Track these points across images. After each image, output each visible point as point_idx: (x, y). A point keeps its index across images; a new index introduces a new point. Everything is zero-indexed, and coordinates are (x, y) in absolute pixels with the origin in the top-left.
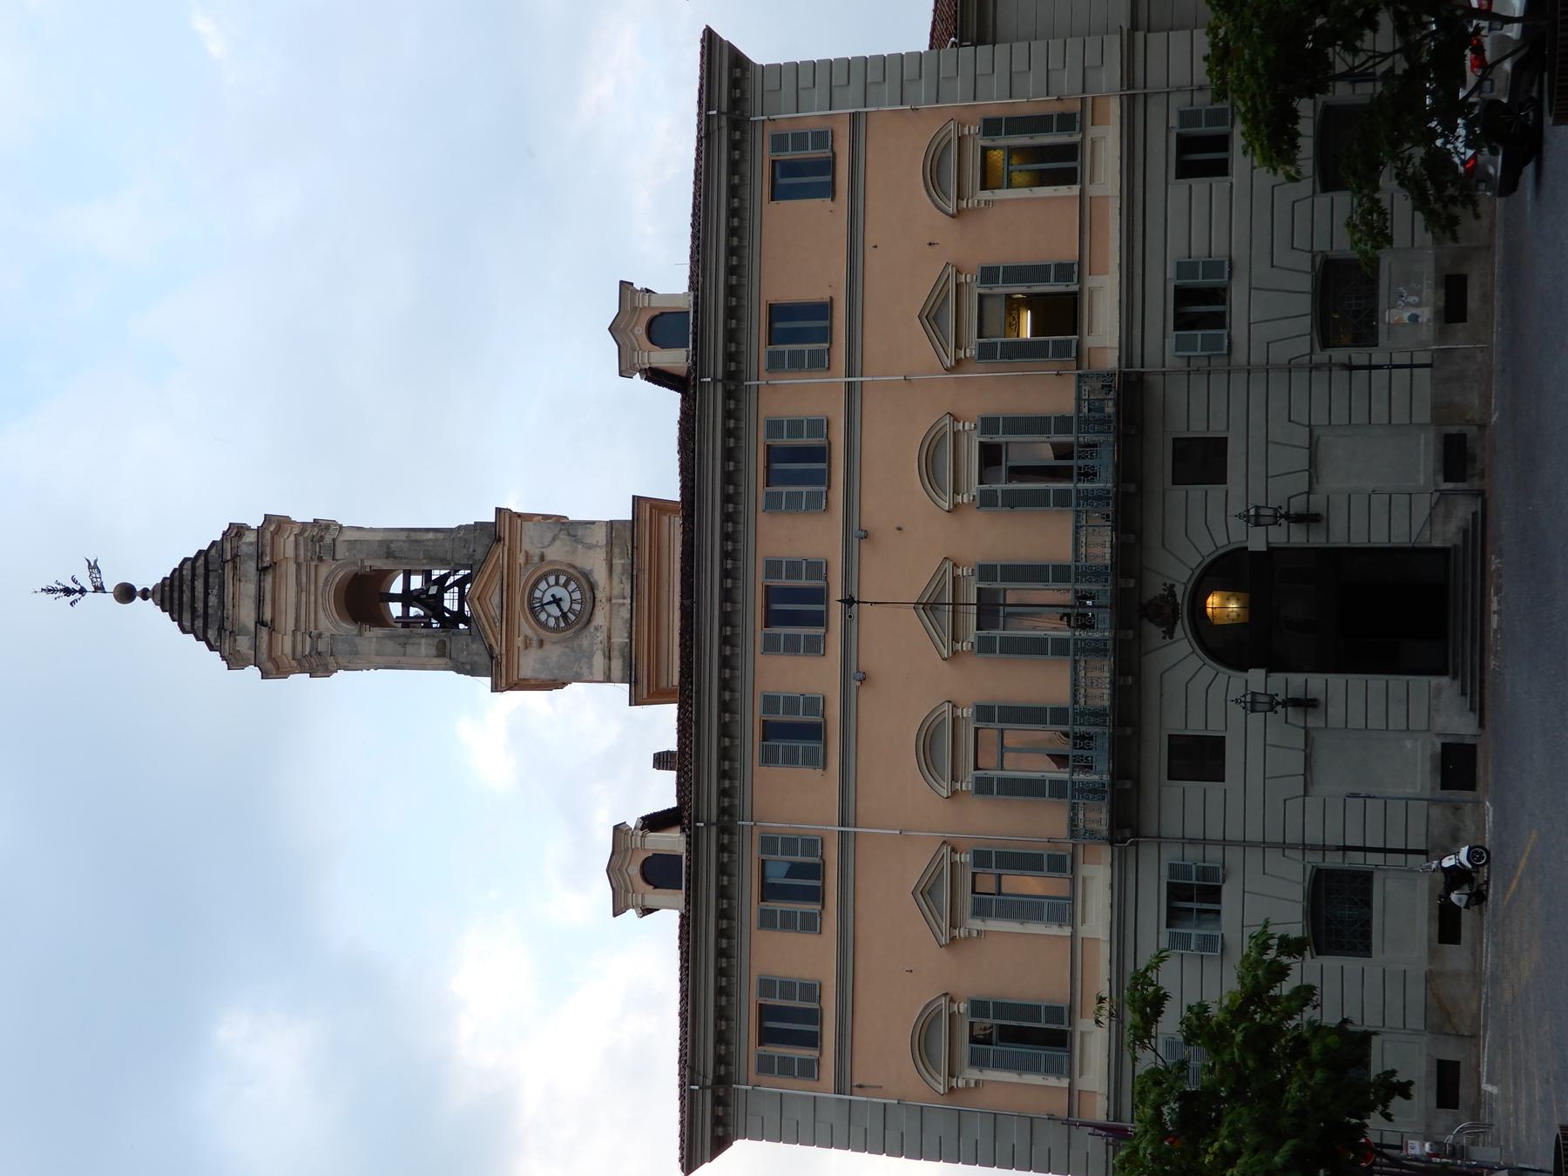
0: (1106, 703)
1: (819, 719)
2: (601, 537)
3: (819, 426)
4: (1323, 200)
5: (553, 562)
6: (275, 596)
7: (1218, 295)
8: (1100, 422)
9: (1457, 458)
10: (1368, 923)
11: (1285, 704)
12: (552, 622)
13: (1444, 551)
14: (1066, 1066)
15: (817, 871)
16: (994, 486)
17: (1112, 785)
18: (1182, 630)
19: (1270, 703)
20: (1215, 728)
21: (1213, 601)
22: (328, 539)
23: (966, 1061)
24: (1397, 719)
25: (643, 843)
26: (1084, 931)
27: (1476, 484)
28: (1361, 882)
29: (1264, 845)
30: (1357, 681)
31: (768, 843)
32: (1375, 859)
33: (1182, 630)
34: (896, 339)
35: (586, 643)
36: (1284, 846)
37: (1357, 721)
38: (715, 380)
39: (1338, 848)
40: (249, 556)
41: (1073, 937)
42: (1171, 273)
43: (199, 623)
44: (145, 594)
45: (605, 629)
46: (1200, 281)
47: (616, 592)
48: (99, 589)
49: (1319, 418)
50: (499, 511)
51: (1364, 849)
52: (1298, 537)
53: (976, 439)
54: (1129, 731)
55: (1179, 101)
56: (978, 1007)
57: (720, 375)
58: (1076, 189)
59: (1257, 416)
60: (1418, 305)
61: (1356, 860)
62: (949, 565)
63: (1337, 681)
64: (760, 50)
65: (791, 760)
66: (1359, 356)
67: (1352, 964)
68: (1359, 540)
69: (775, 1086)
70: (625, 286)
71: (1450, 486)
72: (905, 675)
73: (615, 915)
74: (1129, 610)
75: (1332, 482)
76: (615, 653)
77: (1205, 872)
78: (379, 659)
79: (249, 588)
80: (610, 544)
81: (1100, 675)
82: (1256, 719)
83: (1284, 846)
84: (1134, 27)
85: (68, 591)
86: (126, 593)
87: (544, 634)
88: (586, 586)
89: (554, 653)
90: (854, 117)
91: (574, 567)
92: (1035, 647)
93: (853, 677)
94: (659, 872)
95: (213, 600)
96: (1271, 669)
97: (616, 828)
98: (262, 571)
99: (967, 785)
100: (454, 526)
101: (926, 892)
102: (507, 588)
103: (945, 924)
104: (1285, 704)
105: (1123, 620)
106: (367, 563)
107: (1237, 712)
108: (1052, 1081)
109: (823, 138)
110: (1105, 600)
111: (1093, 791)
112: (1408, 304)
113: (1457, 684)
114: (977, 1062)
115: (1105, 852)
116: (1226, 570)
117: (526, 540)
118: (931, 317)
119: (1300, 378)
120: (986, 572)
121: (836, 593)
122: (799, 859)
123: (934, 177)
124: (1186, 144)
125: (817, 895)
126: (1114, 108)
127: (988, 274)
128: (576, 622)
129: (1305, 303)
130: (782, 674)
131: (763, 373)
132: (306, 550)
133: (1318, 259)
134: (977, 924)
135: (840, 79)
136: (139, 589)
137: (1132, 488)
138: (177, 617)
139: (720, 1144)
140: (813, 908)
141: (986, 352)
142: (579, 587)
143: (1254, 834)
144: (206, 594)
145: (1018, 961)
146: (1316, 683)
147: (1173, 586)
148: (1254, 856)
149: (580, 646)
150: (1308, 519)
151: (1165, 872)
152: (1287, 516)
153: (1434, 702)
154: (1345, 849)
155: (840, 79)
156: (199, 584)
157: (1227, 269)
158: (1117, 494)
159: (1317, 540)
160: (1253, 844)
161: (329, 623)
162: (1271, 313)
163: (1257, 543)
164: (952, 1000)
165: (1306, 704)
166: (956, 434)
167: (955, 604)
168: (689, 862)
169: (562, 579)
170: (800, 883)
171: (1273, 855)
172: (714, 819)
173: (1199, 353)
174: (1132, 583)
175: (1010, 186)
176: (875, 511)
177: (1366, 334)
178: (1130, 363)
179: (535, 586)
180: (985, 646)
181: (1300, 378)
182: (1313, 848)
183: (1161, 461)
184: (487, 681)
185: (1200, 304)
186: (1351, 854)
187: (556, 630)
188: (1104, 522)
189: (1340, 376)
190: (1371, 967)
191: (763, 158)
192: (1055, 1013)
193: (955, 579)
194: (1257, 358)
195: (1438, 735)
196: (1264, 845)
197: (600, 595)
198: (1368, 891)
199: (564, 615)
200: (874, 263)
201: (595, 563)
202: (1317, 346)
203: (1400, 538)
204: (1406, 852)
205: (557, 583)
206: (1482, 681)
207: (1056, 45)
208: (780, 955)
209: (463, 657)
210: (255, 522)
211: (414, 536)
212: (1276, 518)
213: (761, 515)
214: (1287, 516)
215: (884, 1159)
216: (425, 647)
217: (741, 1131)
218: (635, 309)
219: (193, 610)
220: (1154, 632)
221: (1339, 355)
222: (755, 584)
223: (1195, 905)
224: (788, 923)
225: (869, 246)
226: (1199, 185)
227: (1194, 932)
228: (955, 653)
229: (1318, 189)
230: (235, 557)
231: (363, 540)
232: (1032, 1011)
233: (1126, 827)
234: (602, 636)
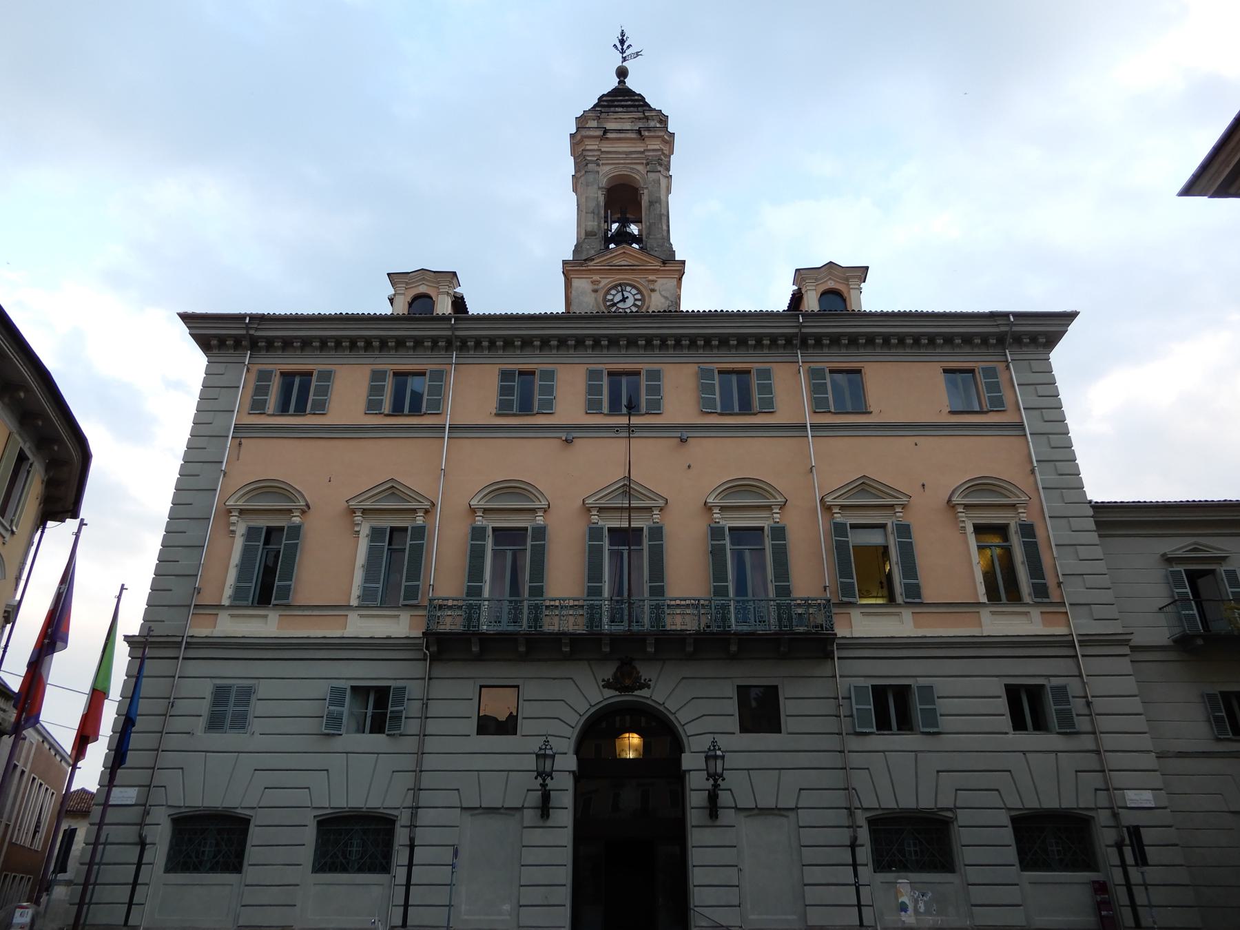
1: (536, 410)
3: (768, 406)
4: (1004, 818)
6: (623, 161)
7: (906, 724)
8: (790, 618)
10: (344, 869)
11: (544, 785)
12: (610, 297)
14: (238, 603)
15: (416, 410)
16: (728, 539)
19: (544, 772)
21: (635, 739)
22: (659, 168)
23: (252, 524)
24: (529, 896)
25: (443, 293)
26: (353, 617)
28: (382, 865)
29: (419, 771)
30: (566, 856)
31: (439, 376)
32: (401, 874)
34: (839, 462)
36: (417, 789)
37: (529, 856)
38: (801, 326)
39: (412, 840)
41: (349, 607)
42: (922, 681)
44: (622, 82)
46: (917, 706)
48: (624, 59)
49: (805, 817)
50: (683, 262)
51: (410, 865)
52: (696, 799)
54: (522, 649)
55: (1074, 687)
56: (296, 531)
57: (804, 330)
58: (984, 599)
60: (916, 911)
61: (400, 857)
62: (661, 503)
63: (565, 837)
64: (1059, 357)
65: (504, 391)
66: (864, 854)
67: (306, 855)
68: (695, 856)
72: (568, 476)
73: (389, 275)
74: (625, 648)
75: (747, 831)
77: (397, 717)
79: (627, 126)
81: (573, 624)
82: (530, 762)
84: (1135, 649)
85: (622, 42)
87: (601, 294)
90: (1021, 426)
92: (594, 572)
93: (569, 434)
94: (421, 302)
96: (578, 777)
97: (454, 274)
98: (639, 131)
99: (480, 521)
101: (393, 489)
103: (368, 505)
104: (544, 785)
105: (615, 639)
107: (535, 745)
108: (228, 592)
110: (635, 628)
112: (916, 902)
114: (251, 533)
116: (662, 731)
117: (664, 281)
118: (864, 485)
119: (839, 798)
120: (657, 533)
121: (635, 420)
122: (425, 397)
123: (980, 486)
124: (1035, 693)
125: (397, 410)
126: (1060, 630)
127: (904, 530)
130: (571, 387)
131: (807, 366)
133: (949, 814)
134: (365, 530)
135: (1049, 415)
137: (734, 648)
138: (609, 94)
139: (204, 343)
140: (387, 407)
141: (839, 529)
143: (429, 762)
144: (622, 106)
145: (333, 563)
146: (564, 817)
147: (649, 687)
148: (408, 762)
150: (713, 808)
152: (716, 786)
154: (412, 847)
155: (1049, 415)
157: (932, 730)
158: (728, 633)
159: (694, 817)
160: (419, 762)
161: (606, 172)
162: (897, 772)
163: (689, 761)
164: (303, 512)
165: (545, 808)
166: (769, 508)
167: (630, 509)
168: (426, 329)
169: (639, 303)
170: (407, 401)
171: (408, 780)
172: (457, 333)
173: (855, 707)
174: (651, 649)
175: (980, 548)
176: (701, 448)
179: (634, 287)
180: (595, 533)
181: (839, 798)
182: (414, 816)
183: (758, 675)
185: (894, 708)
186: (407, 851)
187: (605, 300)
188: (702, 626)
189: (844, 836)
190: (304, 873)
191: (977, 361)
192: (286, 592)
193: (650, 509)
194: (855, 760)
196: (419, 771)
198: (371, 869)
199: (614, 305)
200: (903, 444)
202: (869, 814)
203: (698, 897)
204: (406, 905)
207: (1105, 581)
208: (349, 388)
209: (585, 246)
211: (664, 221)
212: (715, 776)
213: (693, 368)
214: (716, 786)
216: (592, 224)
217: (213, 359)
218: (847, 279)
220: (608, 672)
221: (864, 835)
223: (370, 711)
224: (376, 390)
225: (916, 439)
226: (1002, 705)
227: (345, 710)
228: (589, 510)
229: (1013, 813)
230: (647, 118)
232: (288, 575)
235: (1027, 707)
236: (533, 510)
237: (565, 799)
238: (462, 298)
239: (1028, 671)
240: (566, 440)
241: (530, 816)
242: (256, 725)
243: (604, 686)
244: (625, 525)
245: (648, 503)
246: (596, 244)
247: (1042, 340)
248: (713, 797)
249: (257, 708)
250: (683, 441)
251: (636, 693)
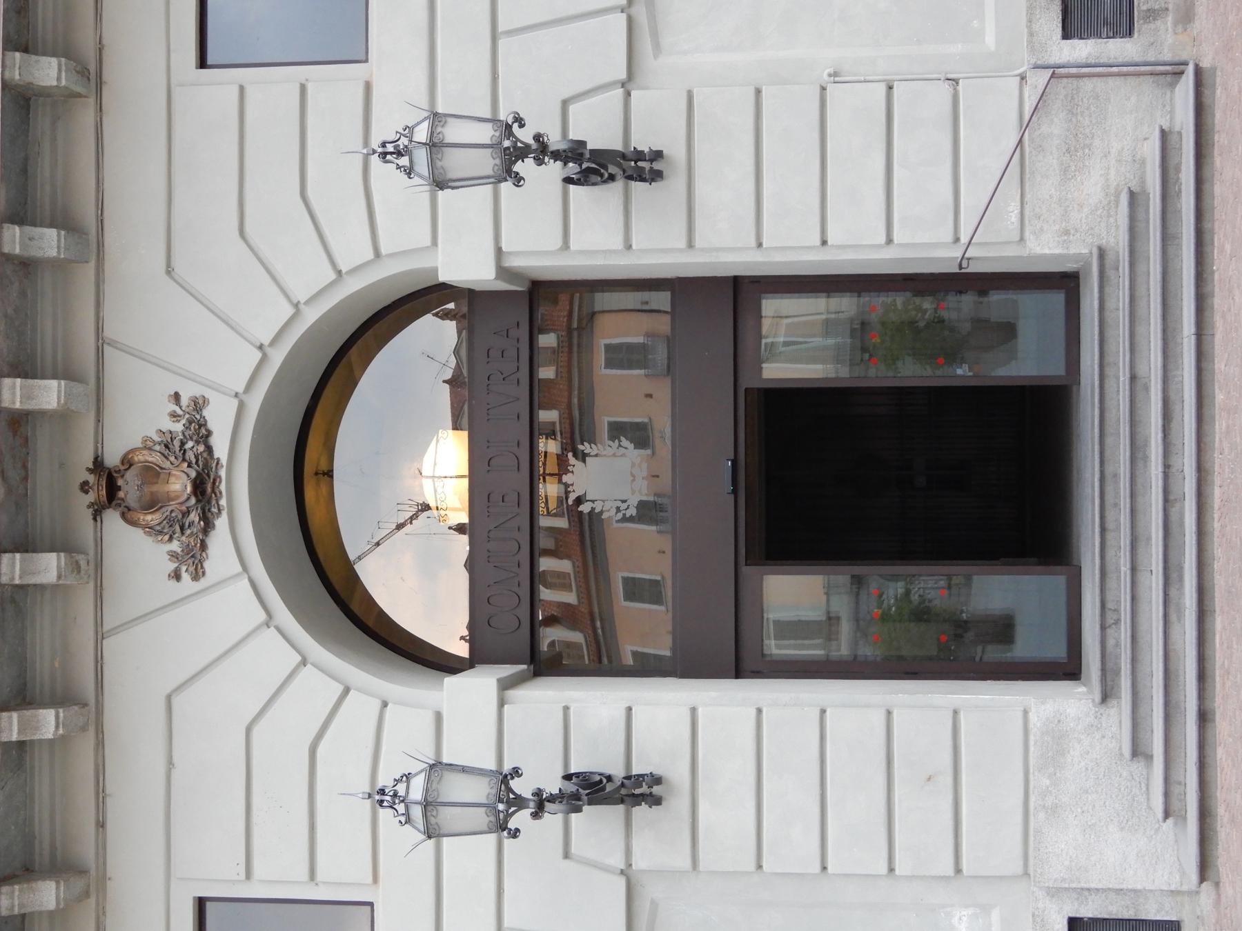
18: (235, 541)
24: (924, 841)
27: (1153, 41)
33: (235, 541)
37: (792, 846)
71: (1082, 50)
137: (47, 72)
147: (198, 404)
153: (1040, 781)
165: (633, 792)
195: (1054, 892)
212: (512, 153)
241: (655, 839)
248: (590, 166)
251: (221, 449)
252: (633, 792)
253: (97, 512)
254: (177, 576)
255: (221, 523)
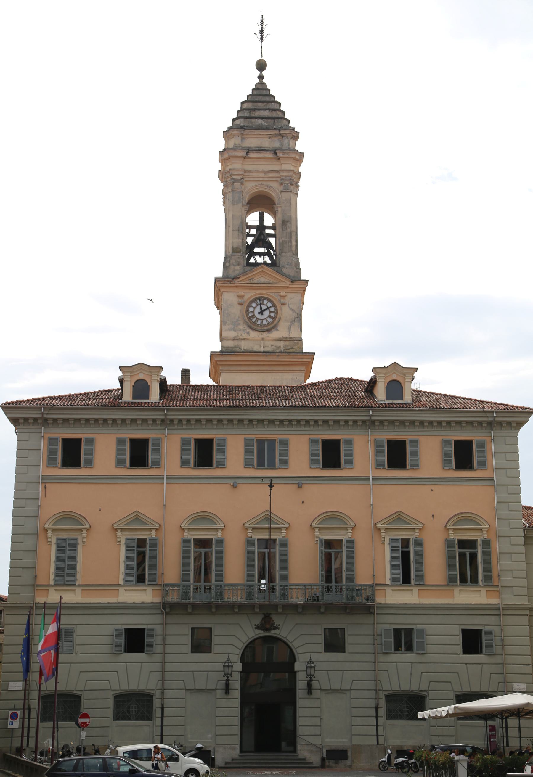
0: (226, 599)
1: (215, 465)
2: (294, 334)
5: (282, 310)
7: (409, 648)
8: (352, 596)
9: (336, 756)
10: (129, 719)
12: (251, 309)
13: (295, 751)
14: (59, 583)
17: (189, 603)
18: (260, 633)
19: (228, 674)
20: (215, 649)
22: (291, 188)
25: (154, 380)
26: (121, 590)
28: (148, 716)
30: (237, 712)
32: (158, 721)
33: (260, 633)
35: (241, 327)
36: (163, 680)
38: (371, 416)
39: (162, 705)
40: (282, 144)
41: (119, 585)
42: (419, 627)
43: (246, 114)
44: (261, 77)
45: (248, 337)
47: (268, 343)
50: (307, 282)
52: (301, 685)
53: (344, 538)
55: (496, 630)
57: (373, 418)
59: (355, 666)
61: (157, 713)
63: (237, 703)
66: (382, 712)
67: (110, 712)
68: (300, 712)
69: (44, 446)
70: (416, 370)
73: (120, 367)
76: (236, 343)
77: (151, 645)
78: (230, 216)
79: (266, 143)
80: (291, 339)
81: (239, 598)
82: (220, 667)
83: (163, 680)
85: (262, 32)
86: (261, 66)
88: (269, 327)
89: (236, 311)
91: (279, 321)
93: (235, 482)
94: (141, 389)
95: (260, 122)
97: (161, 368)
99: (187, 536)
100: (299, 255)
101: (137, 518)
102: (268, 286)
103: (122, 526)
105: (261, 606)
106: (279, 209)
108: (52, 577)
109: (483, 465)
111: (186, 595)
113: (236, 757)
115: (158, 600)
126: (494, 601)
128: (252, 324)
129: (405, 687)
131: (374, 437)
132: (286, 176)
133: (425, 693)
134: (123, 541)
136: (264, 73)
139: (14, 421)
142: (269, 324)
143: (168, 667)
144: (262, 118)
146: (236, 694)
147: (278, 628)
148: (158, 667)
149: (239, 324)
150: (310, 689)
151: (150, 627)
153: (229, 746)
154: (162, 708)
156: (266, 113)
157: (421, 652)
160: (163, 667)
162: (402, 672)
163: (298, 666)
165: (227, 689)
166: (346, 529)
169: (273, 315)
172: (168, 417)
173: (383, 640)
174: (280, 610)
176: (312, 491)
177: (391, 715)
178: (378, 608)
179: (269, 300)
182: (163, 693)
183: (335, 621)
184: (220, 275)
185: (404, 640)
186: (160, 710)
187: (247, 311)
189: (373, 703)
193: (281, 529)
195: (214, 748)
197: (265, 335)
198: (143, 718)
201: (281, 332)
203: (300, 731)
205: (271, 312)
206: (239, 768)
208: (105, 449)
209: (233, 261)
210: (299, 146)
213: (308, 437)
214: (311, 680)
215: (11, 499)
216: (237, 242)
217: (21, 430)
218: (404, 374)
219: (254, 110)
220: (258, 620)
221: (382, 703)
222: (277, 434)
226: (459, 639)
228: (247, 529)
229: (457, 693)
231: (292, 206)
233: (168, 609)
234: (245, 336)
235: (472, 641)
236: (217, 529)
237: (236, 685)
238: (165, 379)
239: (473, 623)
240: (233, 485)
242: (78, 649)
243: (256, 628)
244: (266, 537)
245: (281, 526)
246: (241, 258)
247: (514, 425)
248: (309, 685)
249: (78, 640)
250: (300, 486)
251: (272, 632)
252: (227, 689)
253: (264, 614)
254: (255, 625)
255: (262, 632)
